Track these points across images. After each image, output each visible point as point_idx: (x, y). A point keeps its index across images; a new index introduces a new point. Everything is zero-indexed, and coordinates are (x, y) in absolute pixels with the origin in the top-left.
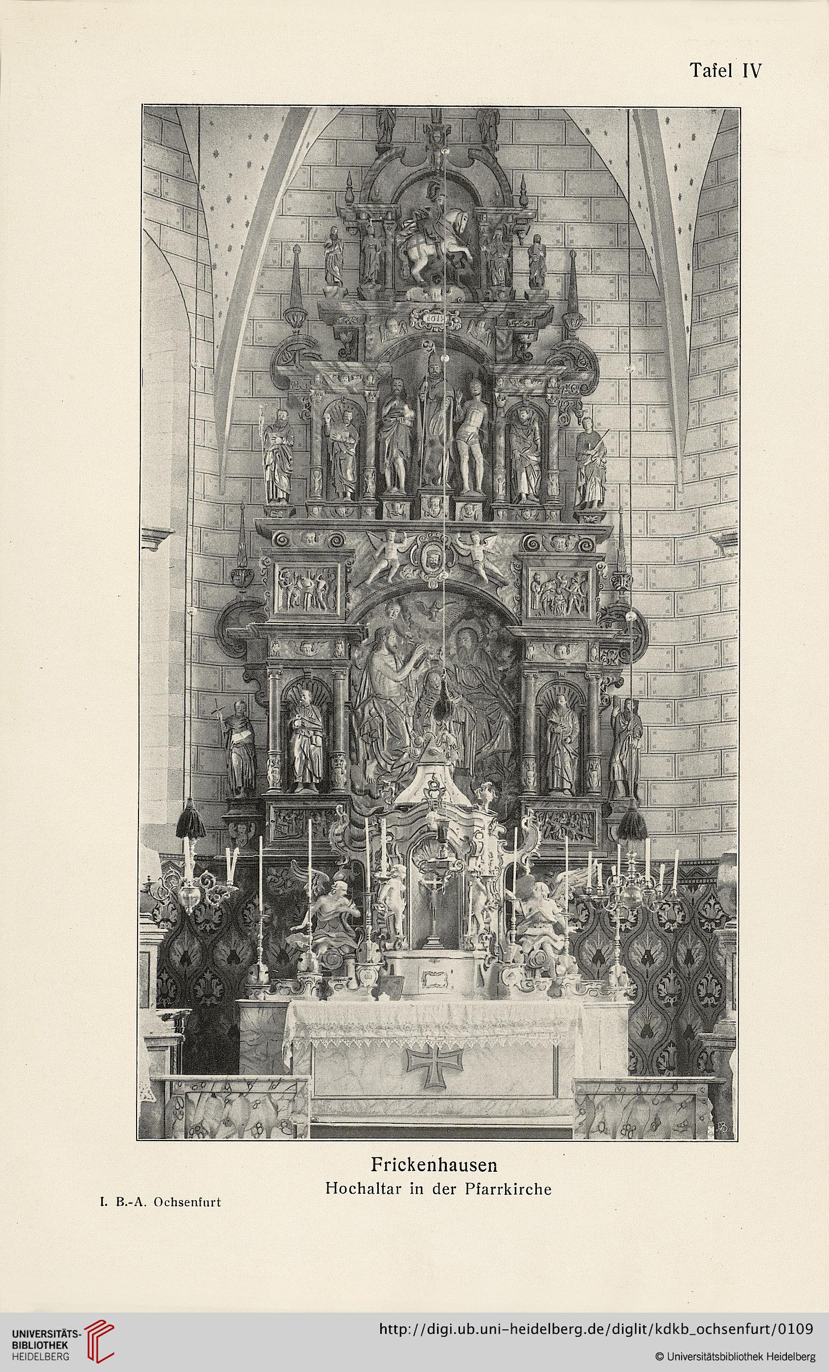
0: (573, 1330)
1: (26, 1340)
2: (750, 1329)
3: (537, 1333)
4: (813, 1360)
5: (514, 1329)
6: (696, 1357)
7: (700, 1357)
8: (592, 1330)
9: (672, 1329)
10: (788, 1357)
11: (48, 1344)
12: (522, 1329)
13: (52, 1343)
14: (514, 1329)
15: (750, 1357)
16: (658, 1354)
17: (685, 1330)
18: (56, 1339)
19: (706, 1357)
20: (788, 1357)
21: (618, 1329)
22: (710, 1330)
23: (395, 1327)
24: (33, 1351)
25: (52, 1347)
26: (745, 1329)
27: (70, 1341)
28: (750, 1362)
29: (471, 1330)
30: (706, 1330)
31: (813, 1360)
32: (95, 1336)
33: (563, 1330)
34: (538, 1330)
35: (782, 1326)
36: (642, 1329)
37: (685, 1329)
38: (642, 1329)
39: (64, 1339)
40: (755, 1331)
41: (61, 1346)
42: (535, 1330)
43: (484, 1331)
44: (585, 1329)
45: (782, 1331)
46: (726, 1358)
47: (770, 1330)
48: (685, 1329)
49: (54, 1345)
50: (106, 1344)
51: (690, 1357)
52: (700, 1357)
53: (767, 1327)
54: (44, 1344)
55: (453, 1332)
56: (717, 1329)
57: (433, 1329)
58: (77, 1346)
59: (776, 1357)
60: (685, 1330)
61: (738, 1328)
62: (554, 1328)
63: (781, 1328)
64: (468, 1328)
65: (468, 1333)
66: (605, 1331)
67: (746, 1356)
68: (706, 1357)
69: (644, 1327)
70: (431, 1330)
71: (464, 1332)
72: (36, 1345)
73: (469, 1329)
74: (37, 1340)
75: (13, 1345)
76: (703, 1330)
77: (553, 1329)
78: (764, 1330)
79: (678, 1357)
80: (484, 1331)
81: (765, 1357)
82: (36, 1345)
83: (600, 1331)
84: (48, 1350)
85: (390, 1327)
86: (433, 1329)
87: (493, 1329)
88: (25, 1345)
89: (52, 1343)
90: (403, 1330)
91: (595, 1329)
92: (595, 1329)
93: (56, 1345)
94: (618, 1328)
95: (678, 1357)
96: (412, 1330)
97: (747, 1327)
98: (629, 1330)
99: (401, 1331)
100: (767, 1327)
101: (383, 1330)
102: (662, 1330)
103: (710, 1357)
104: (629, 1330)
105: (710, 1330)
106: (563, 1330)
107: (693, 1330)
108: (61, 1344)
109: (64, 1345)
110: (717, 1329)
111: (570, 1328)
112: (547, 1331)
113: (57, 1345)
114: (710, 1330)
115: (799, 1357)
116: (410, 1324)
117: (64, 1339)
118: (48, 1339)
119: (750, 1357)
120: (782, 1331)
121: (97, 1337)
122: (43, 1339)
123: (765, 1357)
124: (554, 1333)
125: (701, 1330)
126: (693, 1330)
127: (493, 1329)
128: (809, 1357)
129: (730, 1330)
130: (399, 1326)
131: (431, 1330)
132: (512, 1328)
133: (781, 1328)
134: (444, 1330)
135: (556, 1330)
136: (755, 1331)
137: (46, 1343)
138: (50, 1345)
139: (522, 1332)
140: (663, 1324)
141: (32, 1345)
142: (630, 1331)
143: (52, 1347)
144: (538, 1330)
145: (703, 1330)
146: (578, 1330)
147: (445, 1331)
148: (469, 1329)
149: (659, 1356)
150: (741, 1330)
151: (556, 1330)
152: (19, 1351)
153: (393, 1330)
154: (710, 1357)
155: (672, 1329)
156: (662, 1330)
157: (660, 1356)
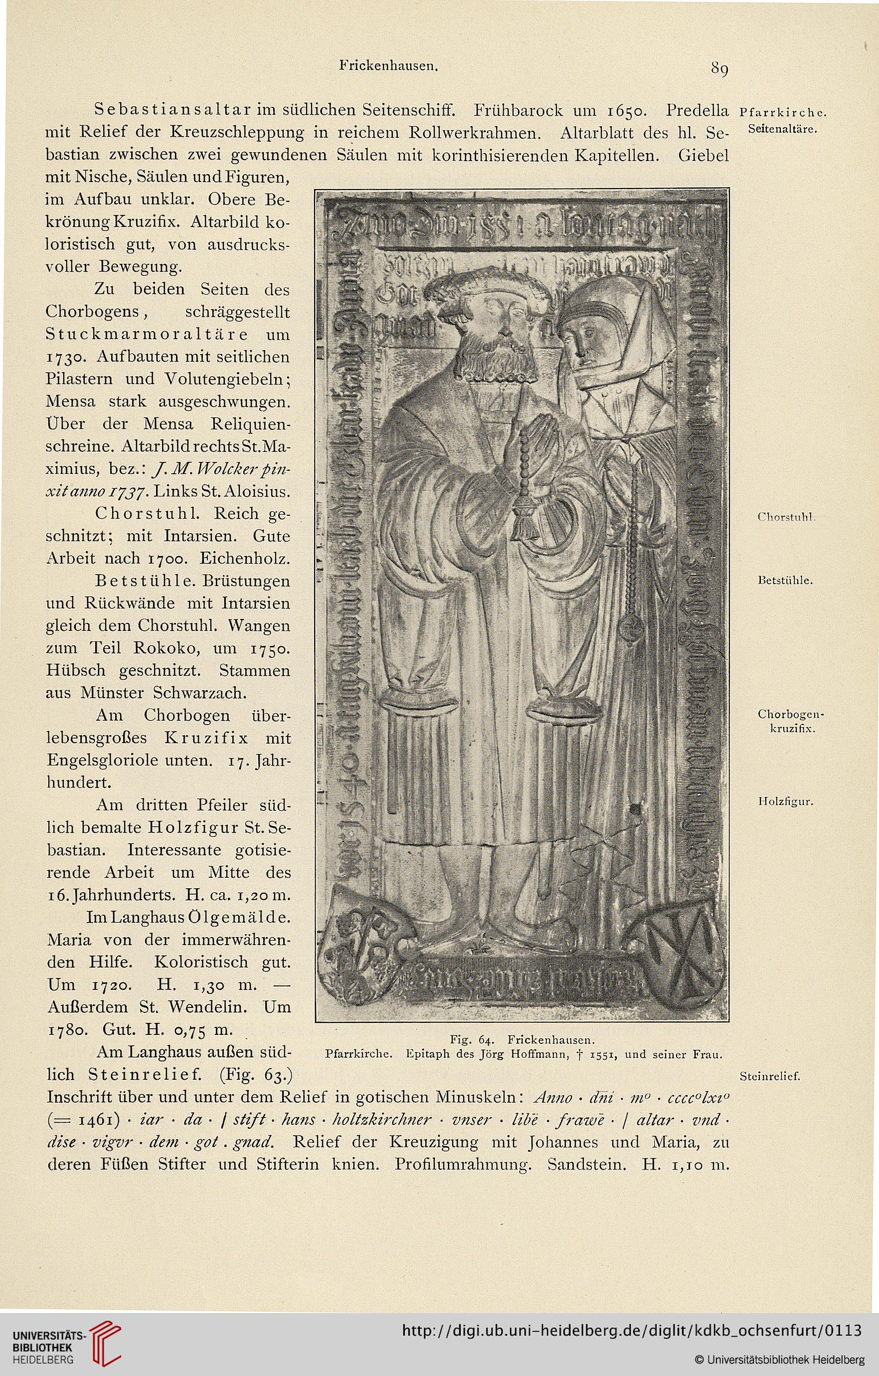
0: (608, 1331)
1: (28, 1342)
2: (795, 1331)
3: (570, 1334)
4: (862, 1363)
5: (545, 1331)
6: (738, 1360)
7: (742, 1361)
8: (627, 1332)
9: (712, 1330)
10: (836, 1360)
11: (51, 1347)
12: (553, 1330)
13: (55, 1346)
14: (545, 1331)
15: (795, 1360)
16: (697, 1357)
17: (726, 1332)
18: (60, 1341)
19: (749, 1360)
20: (836, 1360)
21: (656, 1331)
22: (753, 1332)
23: (419, 1328)
24: (35, 1354)
25: (55, 1349)
26: (790, 1330)
27: (74, 1343)
28: (796, 1366)
29: (499, 1332)
30: (748, 1332)
31: (862, 1363)
32: (101, 1338)
33: (597, 1331)
34: (570, 1331)
35: (829, 1327)
36: (681, 1330)
37: (726, 1331)
38: (681, 1330)
39: (68, 1341)
40: (800, 1333)
41: (65, 1349)
42: (567, 1332)
43: (513, 1333)
44: (620, 1331)
45: (829, 1333)
46: (769, 1361)
47: (817, 1332)
48: (726, 1331)
49: (57, 1348)
50: (112, 1346)
51: (731, 1360)
52: (742, 1361)
53: (813, 1328)
54: (47, 1346)
55: (480, 1334)
56: (760, 1331)
57: (459, 1331)
58: (82, 1349)
59: (822, 1360)
60: (726, 1332)
61: (783, 1329)
62: (587, 1329)
63: (829, 1330)
64: (497, 1329)
65: (497, 1335)
66: (641, 1333)
67: (791, 1359)
68: (749, 1360)
69: (683, 1328)
70: (457, 1332)
71: (492, 1334)
72: (38, 1347)
73: (497, 1331)
74: (40, 1342)
75: (14, 1348)
76: (745, 1332)
77: (588, 1330)
78: (810, 1331)
79: (718, 1360)
80: (513, 1333)
81: (811, 1360)
82: (38, 1347)
83: (636, 1333)
84: (51, 1353)
85: (413, 1328)
86: (459, 1331)
87: (523, 1331)
88: (27, 1348)
89: (55, 1346)
90: (427, 1332)
91: (631, 1331)
92: (631, 1331)
93: (59, 1348)
94: (656, 1329)
95: (718, 1360)
96: (437, 1332)
97: (792, 1328)
98: (667, 1332)
99: (426, 1332)
100: (813, 1328)
101: (407, 1331)
102: (702, 1332)
103: (753, 1360)
104: (667, 1332)
105: (752, 1332)
106: (597, 1331)
107: (734, 1331)
108: (65, 1346)
109: (68, 1347)
110: (760, 1331)
111: (605, 1329)
112: (580, 1333)
113: (61, 1348)
114: (753, 1332)
115: (847, 1361)
116: (435, 1325)
117: (68, 1341)
118: (50, 1342)
119: (795, 1360)
120: (829, 1332)
121: (103, 1339)
122: (46, 1341)
123: (811, 1360)
124: (587, 1335)
125: (743, 1332)
126: (734, 1331)
127: (523, 1331)
128: (858, 1360)
129: (774, 1331)
130: (423, 1327)
131: (457, 1332)
132: (543, 1330)
133: (829, 1330)
134: (471, 1332)
135: (590, 1332)
136: (800, 1333)
137: (49, 1345)
138: (53, 1348)
139: (554, 1333)
140: (703, 1325)
141: (34, 1348)
142: (668, 1333)
143: (55, 1349)
144: (570, 1331)
145: (745, 1332)
146: (613, 1332)
147: (472, 1333)
148: (497, 1331)
149: (699, 1359)
150: (785, 1331)
151: (590, 1332)
152: (20, 1353)
153: (416, 1331)
154: (753, 1360)
155: (712, 1330)
156: (702, 1332)
157: (700, 1359)
